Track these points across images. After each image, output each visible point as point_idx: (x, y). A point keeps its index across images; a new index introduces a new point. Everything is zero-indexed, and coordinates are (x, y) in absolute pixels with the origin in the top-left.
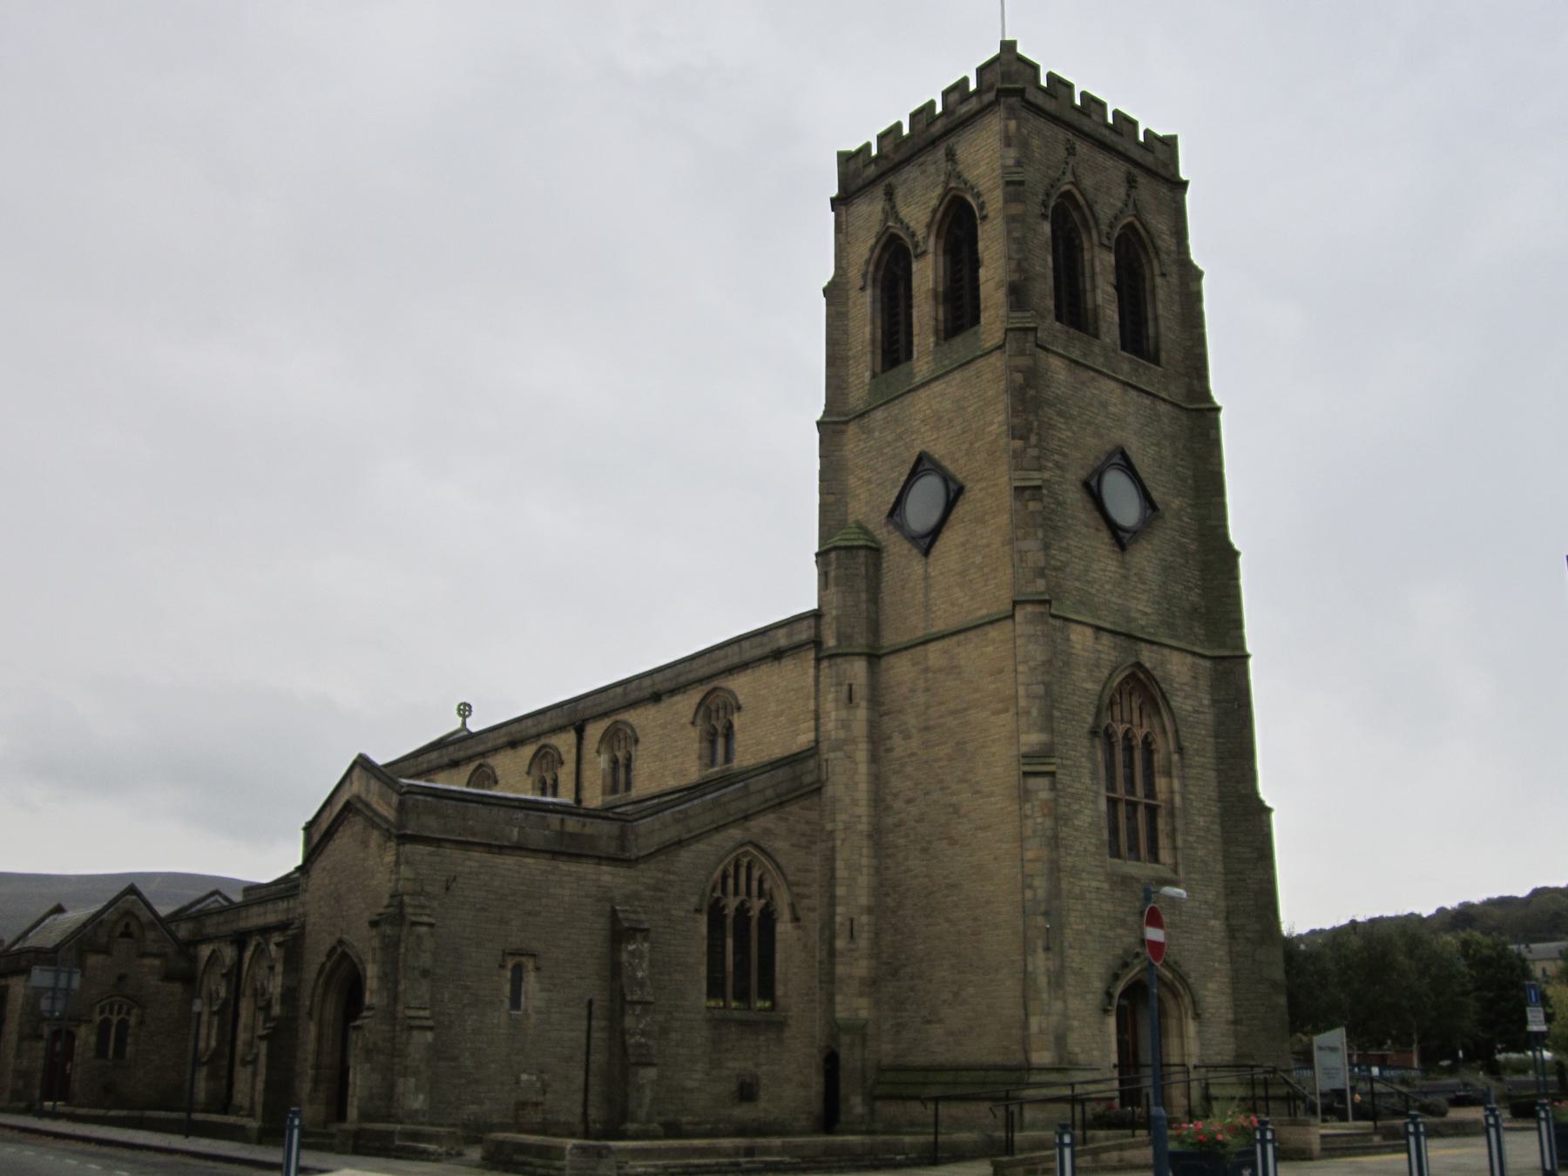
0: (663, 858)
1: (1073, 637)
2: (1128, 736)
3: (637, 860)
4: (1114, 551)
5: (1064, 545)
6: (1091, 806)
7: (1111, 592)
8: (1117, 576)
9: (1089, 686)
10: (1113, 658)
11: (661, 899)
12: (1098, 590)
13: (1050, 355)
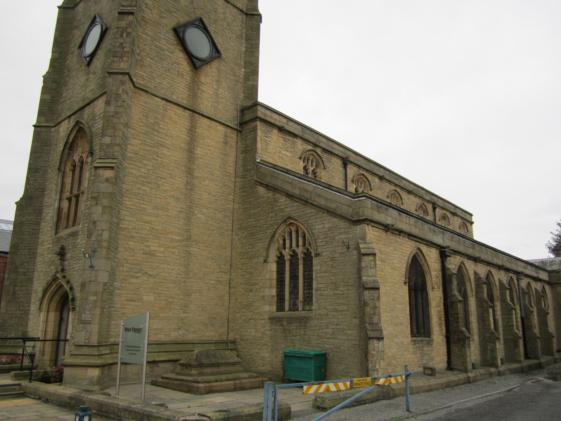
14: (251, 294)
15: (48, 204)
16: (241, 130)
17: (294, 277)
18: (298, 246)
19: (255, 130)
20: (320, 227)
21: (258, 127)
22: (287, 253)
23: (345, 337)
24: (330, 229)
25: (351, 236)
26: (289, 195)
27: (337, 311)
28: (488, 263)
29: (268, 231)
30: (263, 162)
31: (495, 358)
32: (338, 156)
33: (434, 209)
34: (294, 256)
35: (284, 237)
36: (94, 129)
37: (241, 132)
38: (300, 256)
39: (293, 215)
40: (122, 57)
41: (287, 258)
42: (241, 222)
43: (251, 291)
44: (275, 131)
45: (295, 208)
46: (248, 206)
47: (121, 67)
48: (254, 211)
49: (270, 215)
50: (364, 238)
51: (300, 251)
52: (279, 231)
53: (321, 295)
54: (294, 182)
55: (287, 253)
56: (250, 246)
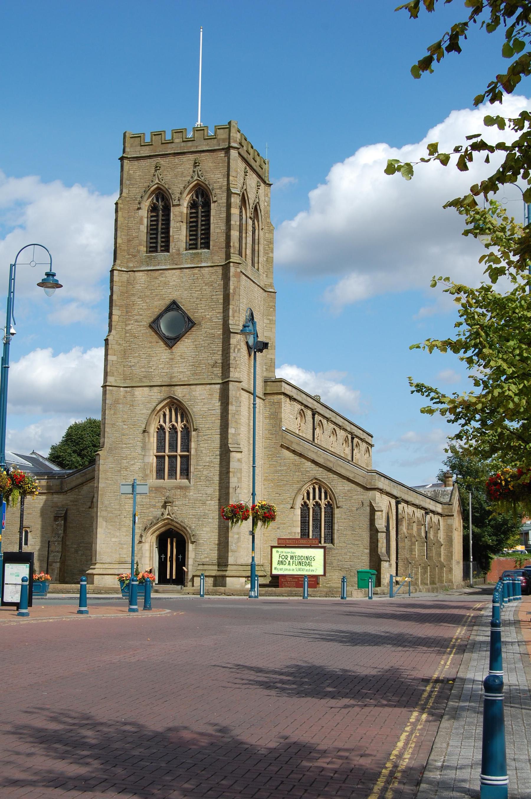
0: (77, 490)
1: (136, 393)
2: (174, 429)
3: (66, 492)
4: (166, 349)
5: (137, 355)
6: (140, 461)
7: (163, 368)
8: (168, 360)
9: (145, 411)
10: (159, 397)
11: (76, 505)
12: (154, 369)
13: (136, 273)
14: (278, 530)
15: (130, 456)
16: (264, 398)
17: (318, 520)
18: (320, 498)
19: (279, 403)
20: (341, 488)
21: (283, 400)
22: (311, 504)
23: (359, 561)
24: (349, 491)
25: (365, 497)
26: (314, 462)
27: (354, 544)
28: (414, 505)
29: (294, 486)
30: (287, 431)
31: (417, 579)
32: (310, 408)
33: (353, 439)
34: (318, 505)
35: (308, 491)
36: (194, 409)
37: (264, 400)
38: (323, 506)
39: (318, 477)
40: (236, 368)
41: (311, 506)
42: (267, 475)
43: (278, 528)
44: (288, 400)
45: (319, 472)
46: (274, 463)
47: (236, 376)
48: (280, 468)
49: (297, 474)
50: (374, 500)
51: (323, 503)
52: (305, 487)
53: (341, 533)
54: (319, 453)
55: (311, 504)
56: (278, 495)
